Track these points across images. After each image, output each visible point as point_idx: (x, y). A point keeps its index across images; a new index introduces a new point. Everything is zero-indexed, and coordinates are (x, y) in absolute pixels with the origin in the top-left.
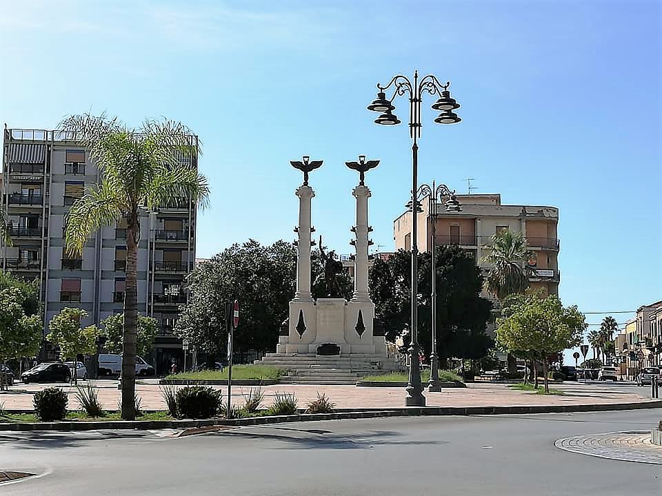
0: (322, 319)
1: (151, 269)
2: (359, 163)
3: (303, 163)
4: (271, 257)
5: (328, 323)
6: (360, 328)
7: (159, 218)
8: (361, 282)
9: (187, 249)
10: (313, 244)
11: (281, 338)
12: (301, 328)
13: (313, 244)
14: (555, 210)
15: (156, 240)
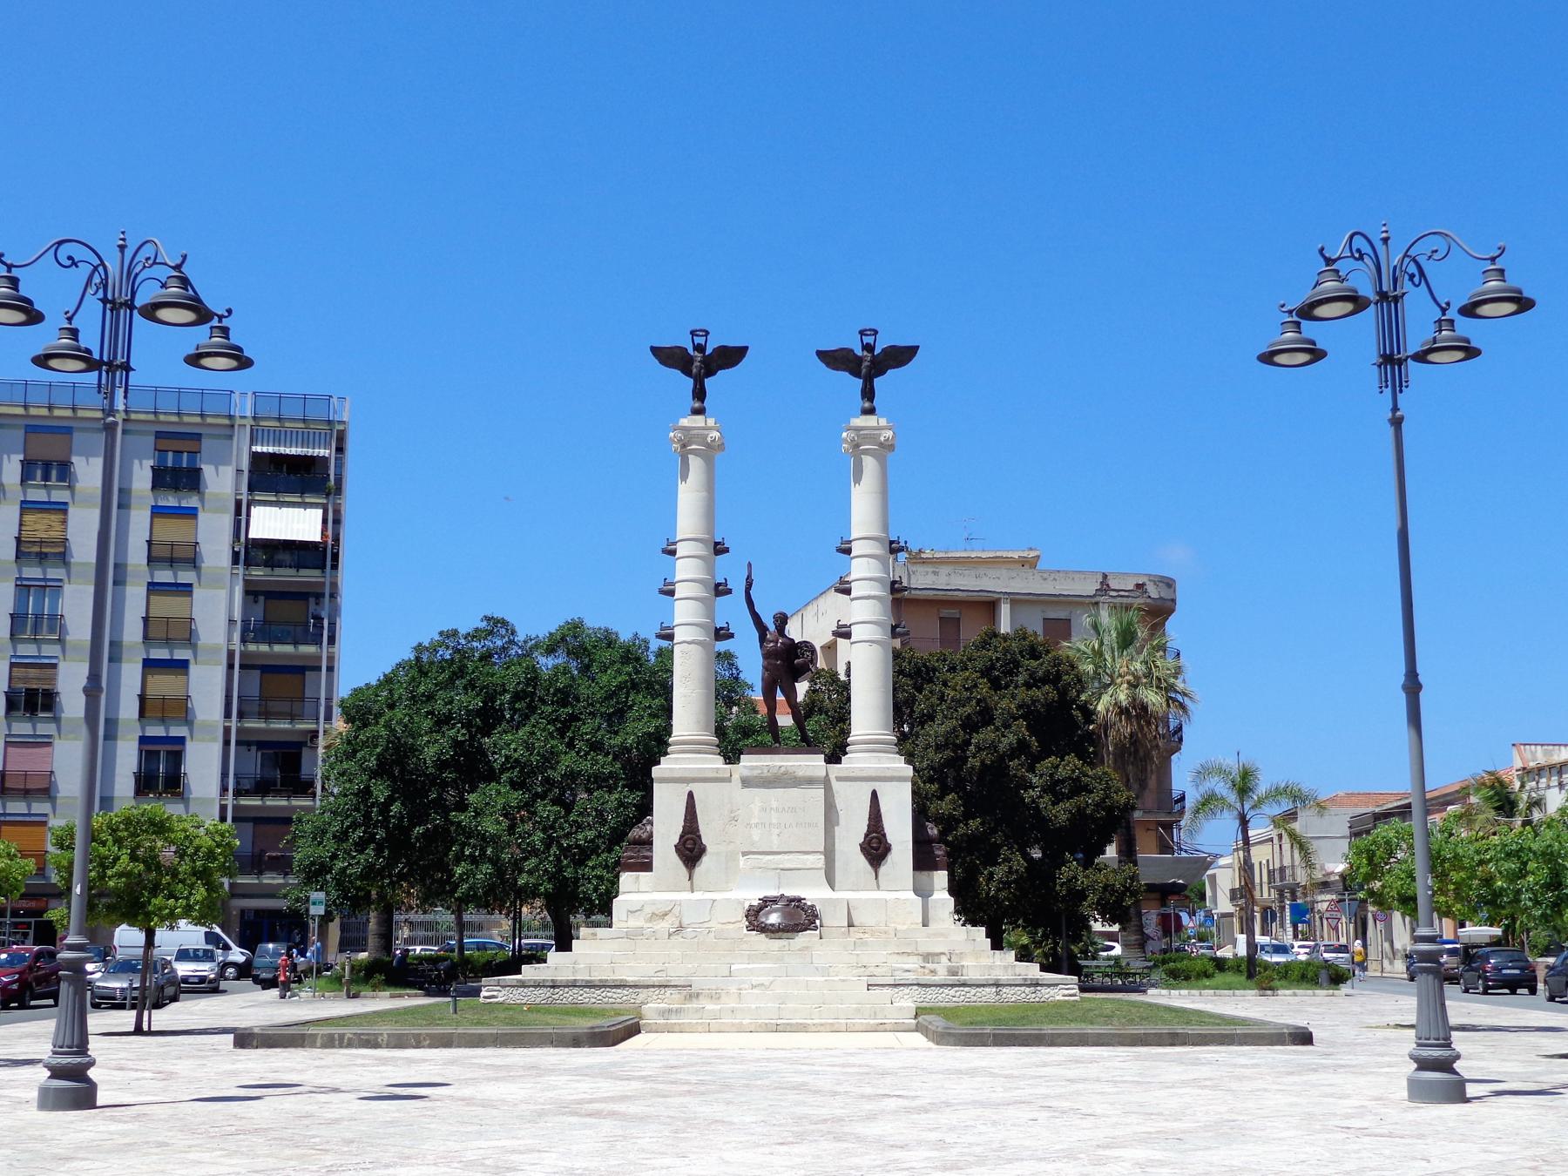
0: (754, 821)
1: (228, 715)
2: (859, 352)
3: (691, 351)
4: (546, 663)
5: (777, 831)
6: (876, 849)
7: (252, 592)
8: (868, 712)
9: (319, 669)
10: (721, 590)
11: (626, 879)
12: (691, 850)
13: (721, 590)
14: (1169, 583)
15: (244, 641)
